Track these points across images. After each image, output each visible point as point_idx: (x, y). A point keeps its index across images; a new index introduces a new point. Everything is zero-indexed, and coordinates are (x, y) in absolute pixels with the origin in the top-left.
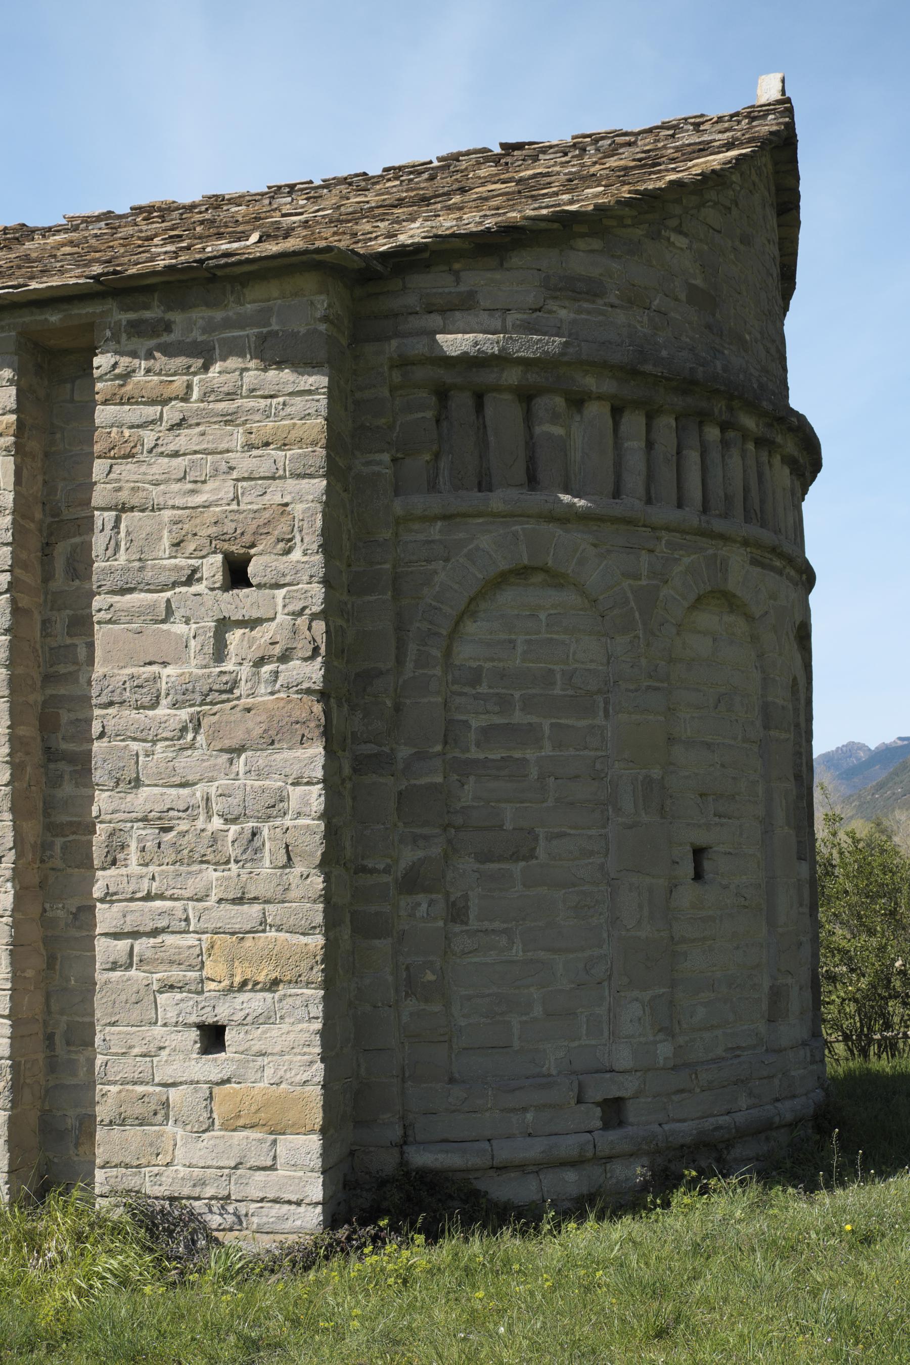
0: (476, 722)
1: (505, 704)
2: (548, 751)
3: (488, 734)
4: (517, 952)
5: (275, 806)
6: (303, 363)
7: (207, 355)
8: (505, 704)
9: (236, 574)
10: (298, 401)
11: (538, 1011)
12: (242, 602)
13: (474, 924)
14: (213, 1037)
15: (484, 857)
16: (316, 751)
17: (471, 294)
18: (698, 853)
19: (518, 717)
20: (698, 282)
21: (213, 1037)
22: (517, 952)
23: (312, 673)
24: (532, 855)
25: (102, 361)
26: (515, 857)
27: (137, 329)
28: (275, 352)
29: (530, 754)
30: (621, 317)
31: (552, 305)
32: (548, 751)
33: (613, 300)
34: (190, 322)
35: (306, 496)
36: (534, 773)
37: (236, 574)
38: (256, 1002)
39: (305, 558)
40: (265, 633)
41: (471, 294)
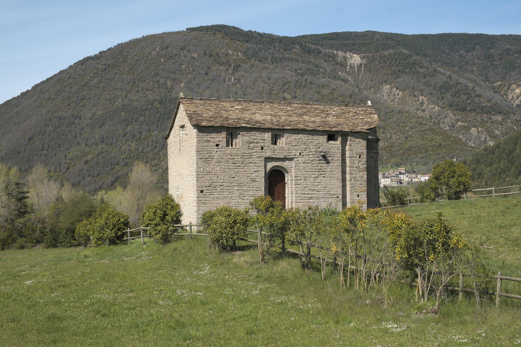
5: (363, 177)
6: (365, 140)
7: (357, 138)
9: (360, 157)
10: (364, 143)
12: (360, 159)
14: (358, 196)
16: (366, 172)
21: (358, 196)
23: (366, 166)
25: (349, 138)
27: (352, 135)
28: (363, 139)
34: (356, 135)
35: (365, 151)
37: (360, 157)
38: (362, 193)
39: (365, 156)
40: (362, 162)
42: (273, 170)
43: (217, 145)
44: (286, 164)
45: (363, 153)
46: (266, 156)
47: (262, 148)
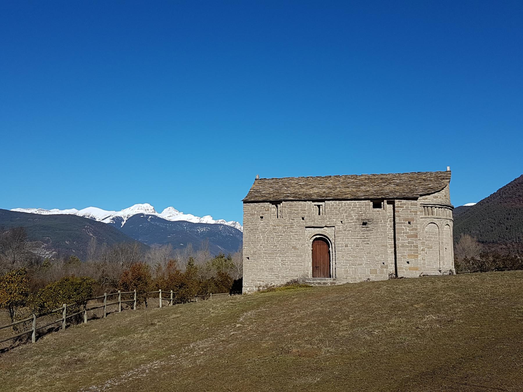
14: (408, 262)
42: (316, 239)
43: (262, 217)
44: (328, 232)
47: (303, 219)
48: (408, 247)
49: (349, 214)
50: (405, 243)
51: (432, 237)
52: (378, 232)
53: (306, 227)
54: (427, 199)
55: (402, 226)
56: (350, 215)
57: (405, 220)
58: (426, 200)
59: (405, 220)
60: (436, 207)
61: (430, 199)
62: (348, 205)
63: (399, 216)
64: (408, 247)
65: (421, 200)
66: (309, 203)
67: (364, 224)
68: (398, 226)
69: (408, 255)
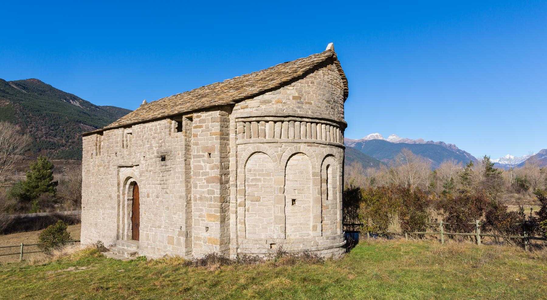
0: (251, 178)
1: (255, 175)
2: (262, 183)
3: (252, 180)
4: (257, 217)
8: (255, 175)
11: (261, 227)
13: (250, 212)
15: (252, 201)
17: (247, 106)
18: (294, 200)
19: (258, 177)
20: (297, 95)
22: (257, 217)
24: (260, 201)
26: (257, 201)
29: (260, 183)
30: (275, 106)
31: (261, 106)
32: (262, 183)
33: (273, 103)
36: (260, 187)
41: (247, 106)
45: (213, 149)
46: (118, 165)
48: (207, 199)
49: (151, 145)
50: (204, 192)
51: (259, 180)
52: (175, 173)
53: (121, 167)
54: (247, 107)
55: (199, 162)
56: (151, 148)
57: (205, 149)
58: (246, 110)
59: (205, 149)
60: (267, 122)
61: (252, 107)
62: (151, 130)
63: (197, 144)
64: (207, 199)
65: (239, 111)
66: (121, 130)
67: (163, 159)
68: (195, 161)
69: (208, 214)
